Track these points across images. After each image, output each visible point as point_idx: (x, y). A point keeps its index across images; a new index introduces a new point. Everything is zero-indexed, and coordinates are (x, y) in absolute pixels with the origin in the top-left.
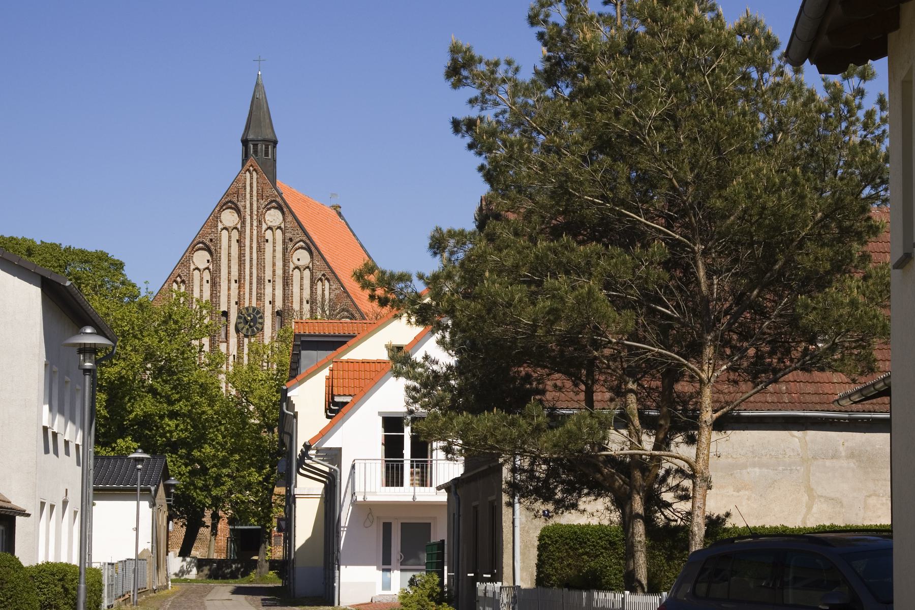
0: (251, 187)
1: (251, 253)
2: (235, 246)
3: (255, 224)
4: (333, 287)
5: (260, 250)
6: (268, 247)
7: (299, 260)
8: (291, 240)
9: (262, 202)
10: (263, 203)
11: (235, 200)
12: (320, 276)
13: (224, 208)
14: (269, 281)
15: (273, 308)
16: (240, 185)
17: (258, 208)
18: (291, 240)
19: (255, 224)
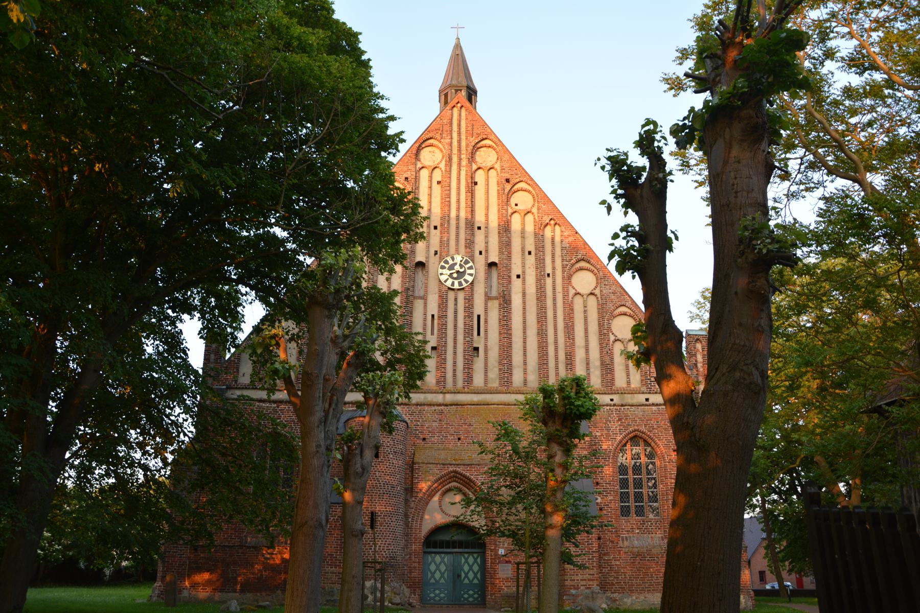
0: (459, 125)
1: (459, 194)
2: (437, 189)
3: (464, 163)
4: (566, 234)
5: (471, 192)
6: (480, 190)
7: (516, 205)
8: (508, 181)
9: (472, 139)
10: (473, 141)
11: (438, 136)
12: (547, 221)
13: (423, 146)
14: (479, 228)
15: (487, 258)
16: (445, 121)
17: (467, 146)
18: (508, 181)
19: (464, 163)
